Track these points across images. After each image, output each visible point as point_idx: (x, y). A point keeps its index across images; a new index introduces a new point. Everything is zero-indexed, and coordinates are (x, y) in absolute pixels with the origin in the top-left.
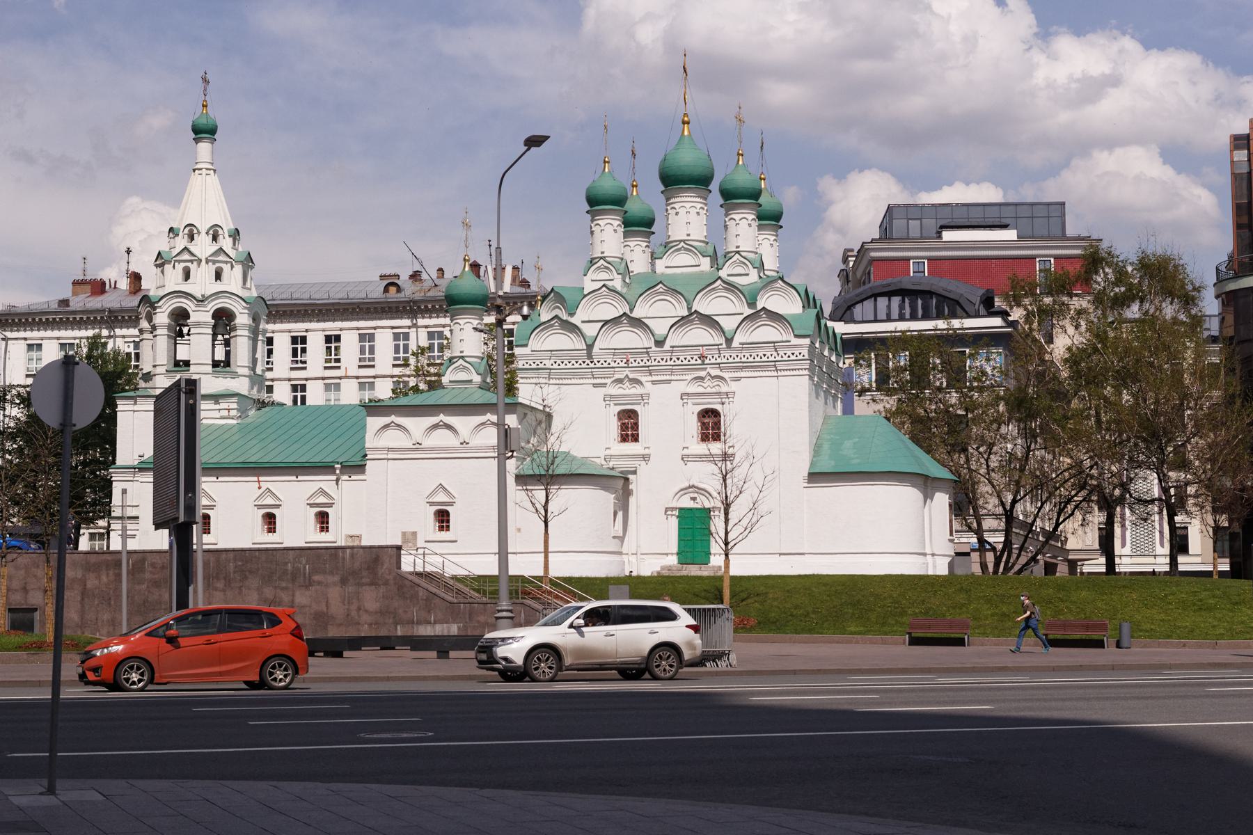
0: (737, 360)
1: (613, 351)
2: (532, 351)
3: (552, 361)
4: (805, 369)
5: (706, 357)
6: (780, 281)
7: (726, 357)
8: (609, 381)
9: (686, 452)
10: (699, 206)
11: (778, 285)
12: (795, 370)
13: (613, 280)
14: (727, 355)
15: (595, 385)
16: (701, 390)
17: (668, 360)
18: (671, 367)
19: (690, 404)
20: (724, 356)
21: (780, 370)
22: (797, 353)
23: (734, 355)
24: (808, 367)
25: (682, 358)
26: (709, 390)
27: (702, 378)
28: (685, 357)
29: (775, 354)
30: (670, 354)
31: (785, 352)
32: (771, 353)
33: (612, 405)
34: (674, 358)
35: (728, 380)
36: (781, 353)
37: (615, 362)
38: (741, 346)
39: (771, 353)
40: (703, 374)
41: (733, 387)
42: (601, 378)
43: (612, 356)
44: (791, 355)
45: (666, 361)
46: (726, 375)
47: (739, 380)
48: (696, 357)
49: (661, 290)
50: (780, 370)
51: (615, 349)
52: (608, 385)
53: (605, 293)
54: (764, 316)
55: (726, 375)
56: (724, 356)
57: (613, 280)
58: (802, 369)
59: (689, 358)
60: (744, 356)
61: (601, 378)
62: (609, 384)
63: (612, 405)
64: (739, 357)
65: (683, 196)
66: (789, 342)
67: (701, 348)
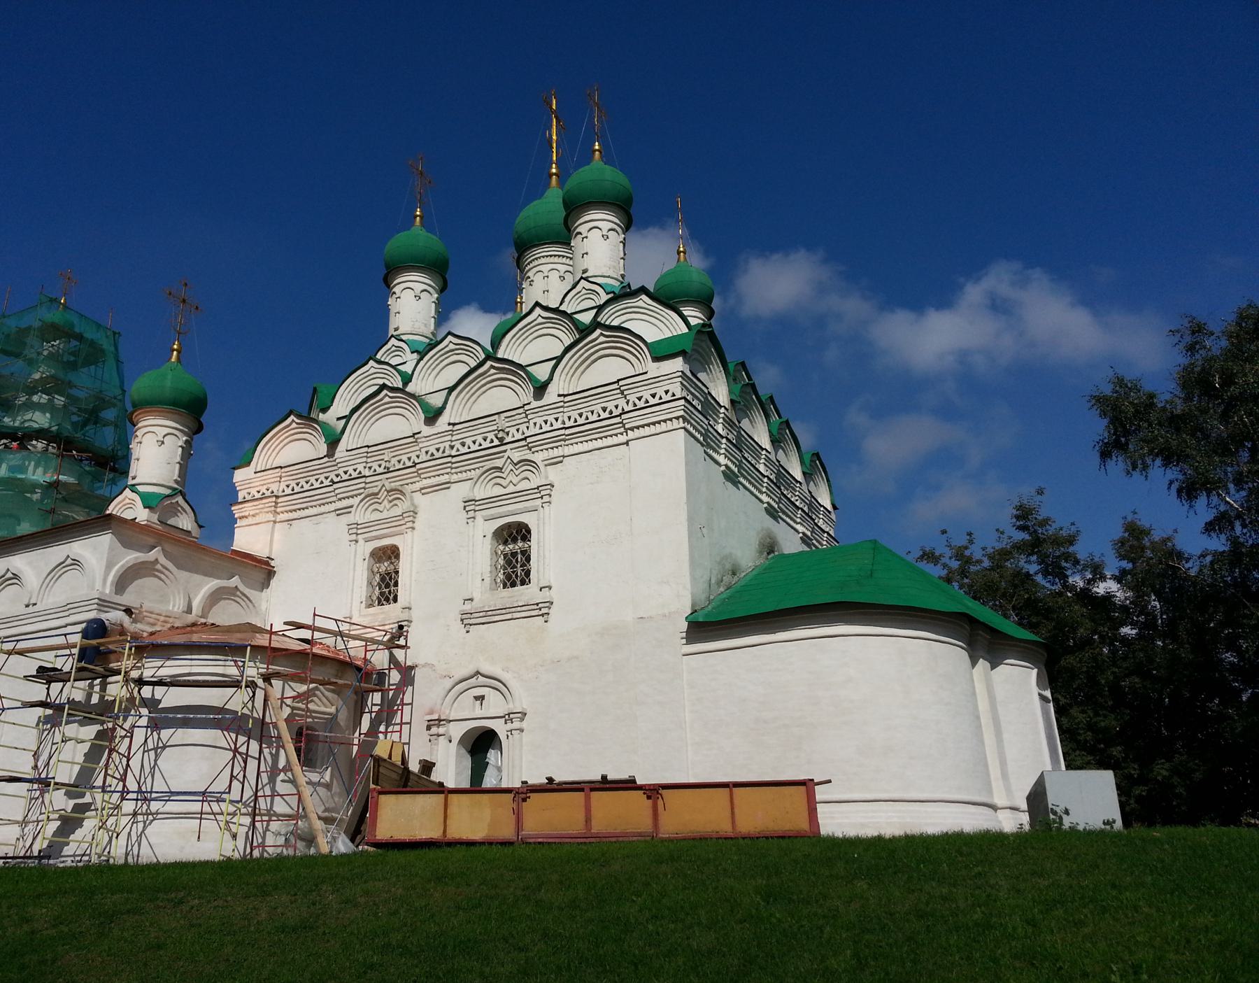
0: (558, 425)
1: (366, 449)
2: (255, 473)
3: (283, 485)
4: (677, 418)
5: (508, 434)
6: (644, 297)
7: (538, 426)
8: (356, 501)
9: (468, 607)
10: (563, 268)
11: (640, 304)
12: (659, 422)
13: (405, 363)
14: (540, 421)
15: (339, 512)
16: (498, 491)
17: (448, 447)
18: (449, 459)
19: (479, 519)
20: (535, 424)
21: (632, 429)
22: (660, 392)
23: (551, 419)
24: (682, 413)
25: (469, 441)
26: (511, 489)
27: (500, 469)
28: (473, 439)
29: (622, 403)
30: (449, 438)
31: (639, 395)
32: (615, 403)
33: (361, 542)
34: (458, 445)
35: (541, 465)
36: (632, 398)
37: (370, 468)
38: (562, 399)
39: (615, 403)
40: (499, 463)
41: (553, 474)
42: (348, 498)
43: (364, 459)
44: (650, 399)
45: (444, 452)
46: (538, 457)
47: (561, 462)
48: (491, 436)
49: (452, 346)
50: (632, 429)
51: (368, 447)
52: (355, 507)
53: (373, 370)
54: (602, 339)
55: (538, 457)
56: (535, 424)
57: (405, 363)
58: (671, 420)
59: (479, 439)
60: (569, 418)
61: (348, 498)
62: (355, 507)
63: (361, 542)
64: (560, 421)
65: (540, 258)
66: (646, 373)
67: (496, 417)
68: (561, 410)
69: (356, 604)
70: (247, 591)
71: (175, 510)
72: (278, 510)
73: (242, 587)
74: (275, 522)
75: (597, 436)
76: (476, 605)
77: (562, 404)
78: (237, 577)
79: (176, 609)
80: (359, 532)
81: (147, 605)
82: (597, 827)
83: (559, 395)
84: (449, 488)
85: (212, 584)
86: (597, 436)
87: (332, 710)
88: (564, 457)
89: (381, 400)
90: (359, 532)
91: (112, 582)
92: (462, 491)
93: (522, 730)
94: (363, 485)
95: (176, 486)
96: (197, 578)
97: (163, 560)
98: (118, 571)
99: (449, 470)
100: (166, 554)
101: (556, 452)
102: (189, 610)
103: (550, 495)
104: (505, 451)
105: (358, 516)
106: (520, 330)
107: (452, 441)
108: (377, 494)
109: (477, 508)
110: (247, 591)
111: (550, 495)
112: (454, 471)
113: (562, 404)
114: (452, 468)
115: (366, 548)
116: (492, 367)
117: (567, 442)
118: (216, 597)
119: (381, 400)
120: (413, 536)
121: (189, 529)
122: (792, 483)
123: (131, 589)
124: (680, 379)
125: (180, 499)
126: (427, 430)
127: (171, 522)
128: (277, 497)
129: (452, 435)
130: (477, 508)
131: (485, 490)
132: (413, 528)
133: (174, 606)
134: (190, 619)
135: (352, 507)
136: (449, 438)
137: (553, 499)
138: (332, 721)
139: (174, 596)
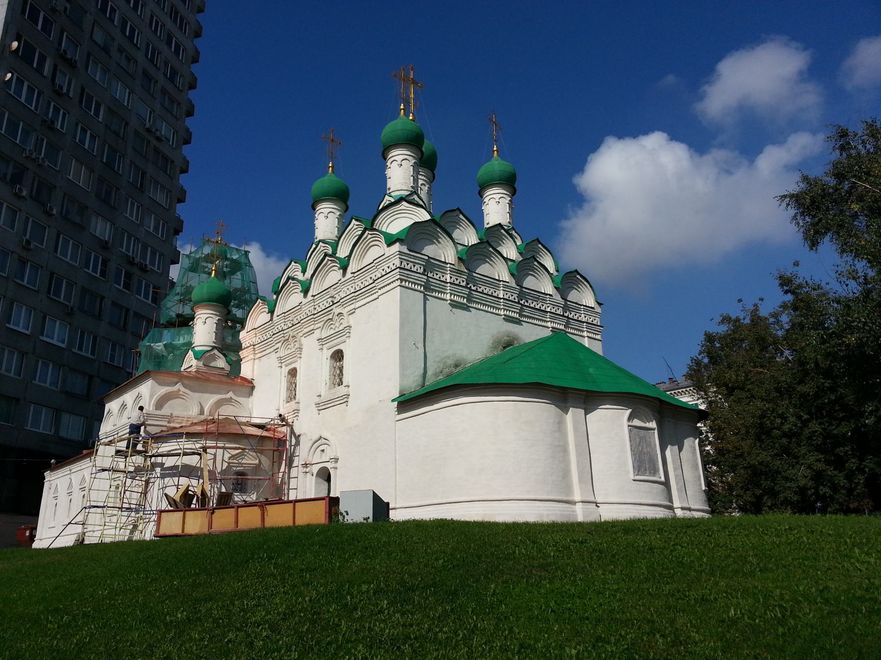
1: (283, 315)
4: (397, 280)
6: (404, 203)
8: (279, 345)
11: (402, 207)
16: (332, 332)
24: (398, 277)
26: (337, 330)
27: (331, 319)
30: (313, 304)
38: (352, 275)
40: (330, 317)
41: (352, 320)
43: (284, 320)
46: (345, 311)
47: (354, 312)
51: (284, 313)
63: (284, 367)
67: (329, 290)
68: (353, 281)
69: (282, 400)
70: (238, 399)
71: (214, 358)
72: (256, 352)
73: (234, 397)
74: (254, 359)
75: (368, 295)
76: (323, 399)
77: (353, 278)
78: (231, 392)
79: (193, 414)
80: (282, 361)
81: (175, 413)
82: (299, 522)
83: (352, 273)
84: (313, 333)
85: (215, 398)
86: (368, 295)
87: (257, 462)
88: (355, 309)
89: (289, 286)
90: (282, 361)
91: (153, 404)
92: (317, 334)
93: (336, 468)
94: (282, 335)
95: (214, 345)
96: (206, 395)
97: (182, 389)
98: (156, 398)
99: (313, 322)
100: (185, 386)
101: (352, 307)
102: (202, 412)
103: (350, 333)
104: (332, 310)
105: (282, 353)
106: (347, 234)
107: (314, 306)
108: (288, 339)
109: (324, 343)
110: (238, 399)
111: (350, 333)
112: (316, 323)
113: (353, 278)
114: (315, 321)
115: (286, 370)
116: (328, 260)
117: (357, 300)
118: (219, 404)
119: (289, 286)
120: (301, 362)
121: (223, 366)
122: (540, 296)
123: (166, 406)
124: (398, 256)
125: (216, 352)
126: (305, 301)
127: (212, 364)
128: (254, 345)
129: (314, 302)
130: (324, 343)
131: (325, 333)
132: (300, 357)
133: (193, 412)
134: (202, 417)
135: (278, 348)
136: (313, 304)
137: (351, 335)
138: (257, 468)
139: (193, 408)
